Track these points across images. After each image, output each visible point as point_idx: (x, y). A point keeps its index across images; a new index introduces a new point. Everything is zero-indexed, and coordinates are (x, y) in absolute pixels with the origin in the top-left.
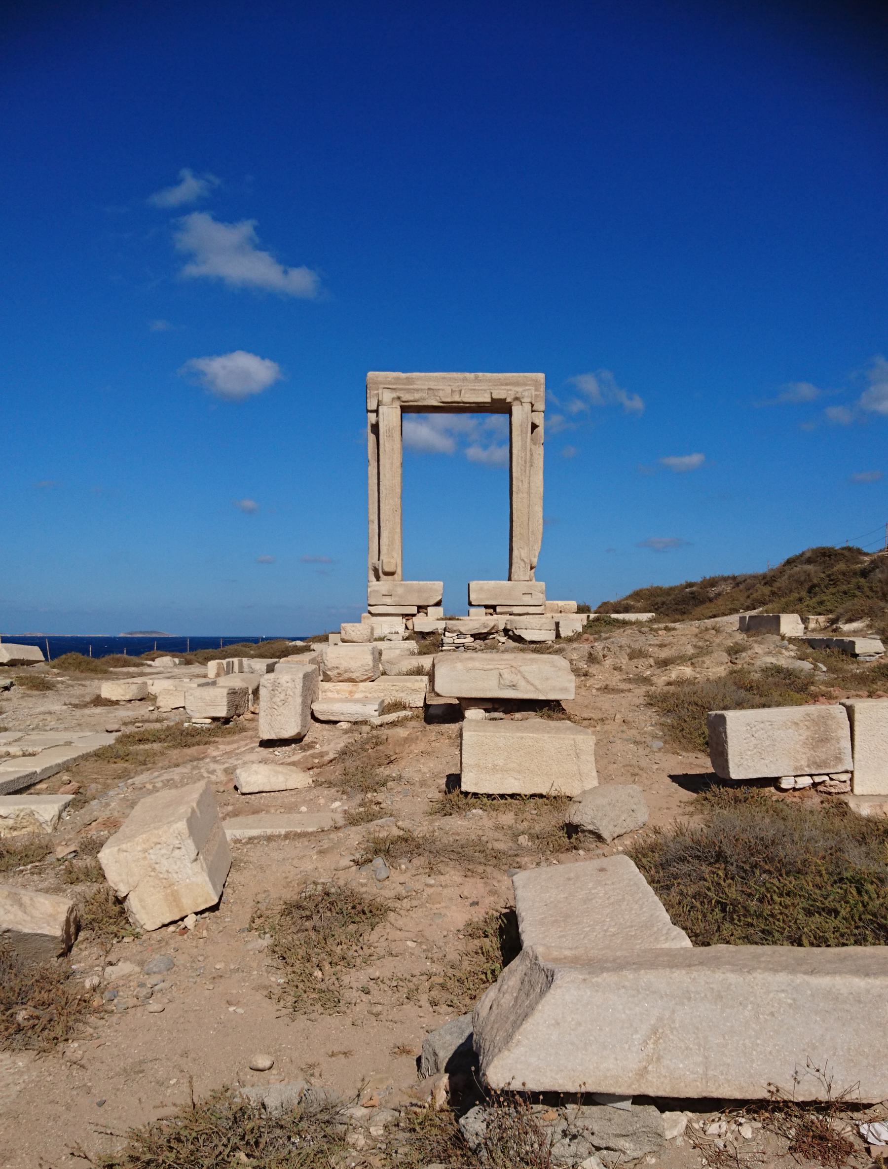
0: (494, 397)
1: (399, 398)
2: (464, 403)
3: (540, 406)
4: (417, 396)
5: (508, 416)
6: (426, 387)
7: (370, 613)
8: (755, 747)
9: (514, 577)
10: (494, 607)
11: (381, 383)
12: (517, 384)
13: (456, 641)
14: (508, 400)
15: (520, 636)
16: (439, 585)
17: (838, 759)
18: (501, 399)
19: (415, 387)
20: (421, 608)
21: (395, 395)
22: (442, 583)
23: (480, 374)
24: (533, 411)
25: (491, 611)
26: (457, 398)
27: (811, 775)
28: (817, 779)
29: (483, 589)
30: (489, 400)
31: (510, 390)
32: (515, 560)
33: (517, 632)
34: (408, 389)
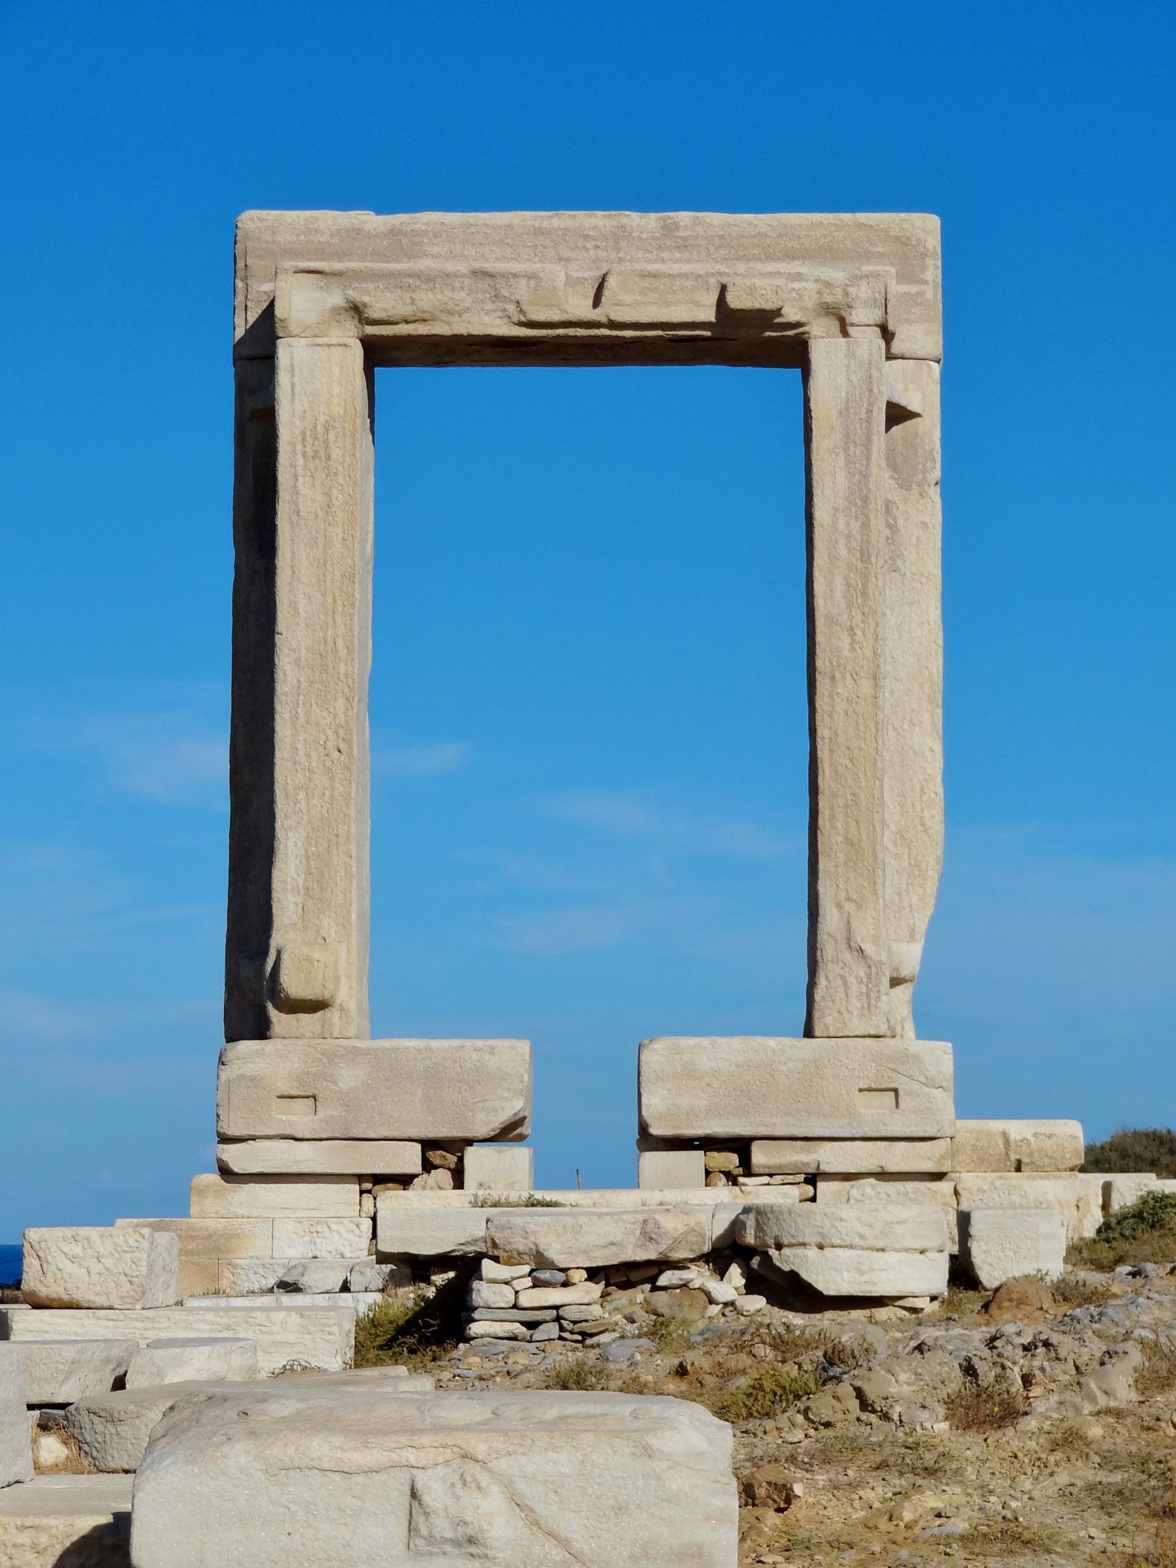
0: (735, 301)
1: (357, 310)
2: (612, 325)
3: (923, 335)
4: (426, 299)
5: (798, 371)
6: (462, 267)
7: (226, 1172)
9: (825, 1020)
10: (741, 1146)
12: (829, 253)
13: (526, 1300)
14: (791, 314)
15: (794, 1276)
16: (511, 1056)
18: (762, 312)
19: (421, 265)
20: (444, 1153)
21: (337, 299)
22: (524, 1046)
23: (684, 217)
24: (890, 357)
25: (731, 1160)
26: (581, 308)
30: (709, 315)
31: (799, 277)
32: (828, 948)
33: (784, 1260)
34: (392, 275)
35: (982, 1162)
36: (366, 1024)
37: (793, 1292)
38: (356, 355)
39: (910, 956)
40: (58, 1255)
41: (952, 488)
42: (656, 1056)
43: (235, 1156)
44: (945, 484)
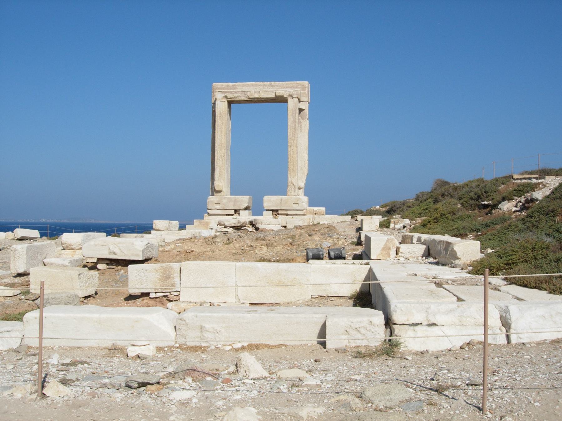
0: (277, 94)
1: (226, 97)
4: (235, 95)
8: (139, 279)
9: (289, 193)
10: (277, 211)
11: (219, 89)
14: (285, 96)
17: (173, 286)
19: (237, 90)
20: (236, 211)
21: (224, 95)
23: (273, 83)
26: (257, 96)
27: (163, 292)
28: (165, 294)
29: (270, 201)
30: (274, 96)
35: (310, 213)
36: (229, 193)
37: (257, 229)
38: (226, 103)
39: (302, 184)
40: (158, 224)
41: (309, 119)
42: (266, 198)
43: (209, 211)
44: (309, 119)
